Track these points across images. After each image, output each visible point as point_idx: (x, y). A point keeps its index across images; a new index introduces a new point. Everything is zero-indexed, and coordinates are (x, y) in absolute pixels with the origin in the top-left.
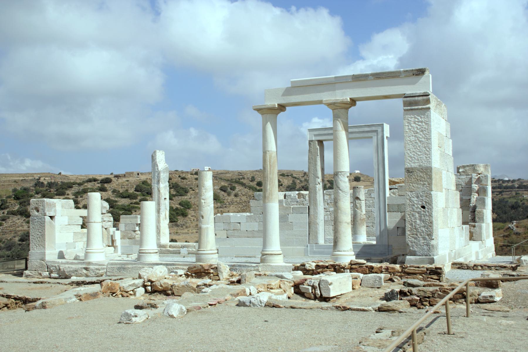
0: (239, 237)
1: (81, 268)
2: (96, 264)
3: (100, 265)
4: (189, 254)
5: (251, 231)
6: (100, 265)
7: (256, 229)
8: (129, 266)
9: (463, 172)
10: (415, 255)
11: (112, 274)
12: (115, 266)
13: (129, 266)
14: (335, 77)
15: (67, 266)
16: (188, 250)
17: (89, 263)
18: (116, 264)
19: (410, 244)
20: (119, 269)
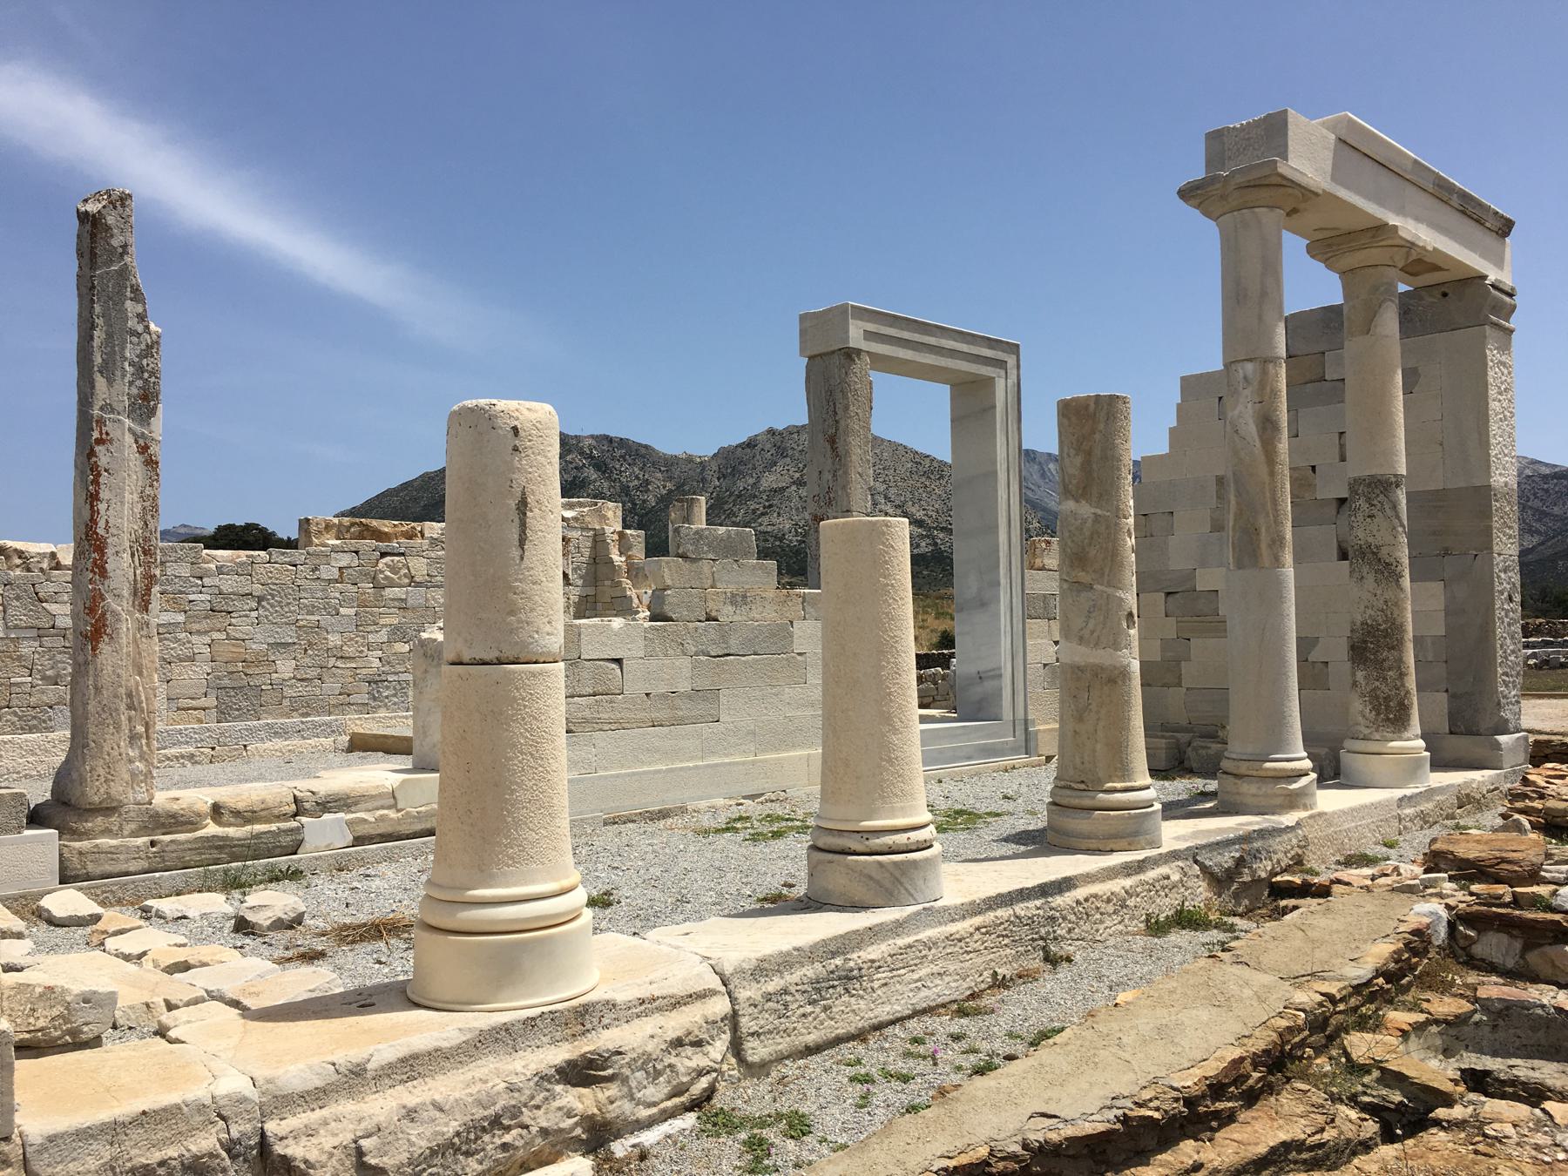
0: (620, 725)
1: (543, 1078)
2: (647, 1006)
3: (677, 1003)
4: (359, 841)
5: (663, 696)
6: (677, 1003)
7: (684, 687)
8: (875, 952)
9: (575, 519)
10: (1505, 732)
11: (784, 1044)
12: (792, 978)
13: (875, 952)
14: (1416, 161)
15: (381, 1105)
16: (349, 824)
17: (583, 1017)
18: (785, 962)
19: (1503, 701)
20: (817, 990)
